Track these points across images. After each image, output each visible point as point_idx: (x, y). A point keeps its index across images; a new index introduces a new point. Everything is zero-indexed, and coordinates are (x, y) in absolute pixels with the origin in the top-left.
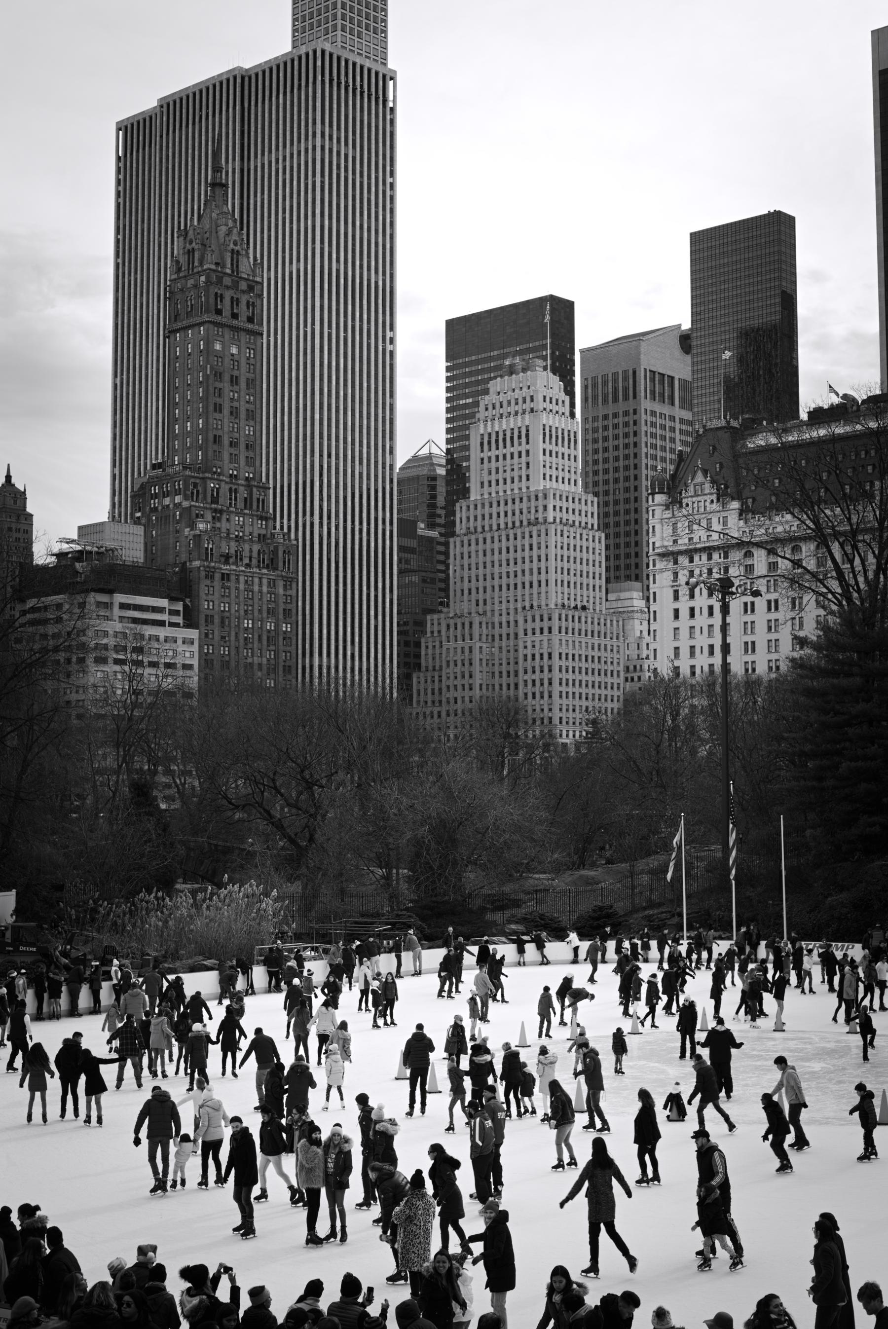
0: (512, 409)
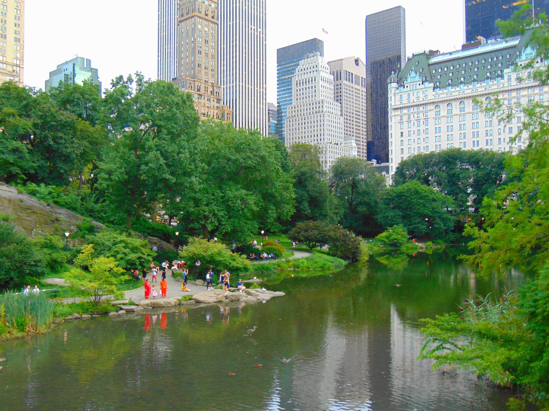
0: (309, 70)
